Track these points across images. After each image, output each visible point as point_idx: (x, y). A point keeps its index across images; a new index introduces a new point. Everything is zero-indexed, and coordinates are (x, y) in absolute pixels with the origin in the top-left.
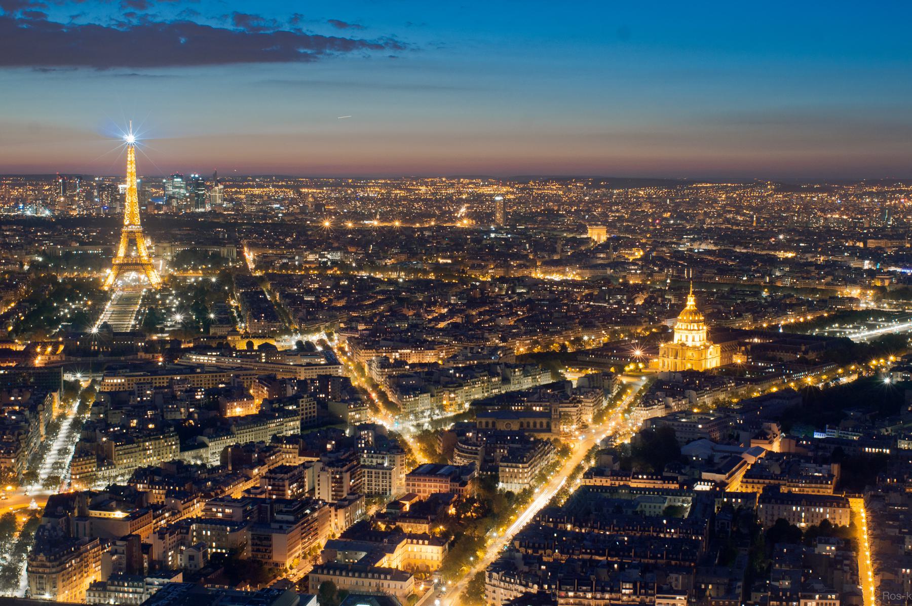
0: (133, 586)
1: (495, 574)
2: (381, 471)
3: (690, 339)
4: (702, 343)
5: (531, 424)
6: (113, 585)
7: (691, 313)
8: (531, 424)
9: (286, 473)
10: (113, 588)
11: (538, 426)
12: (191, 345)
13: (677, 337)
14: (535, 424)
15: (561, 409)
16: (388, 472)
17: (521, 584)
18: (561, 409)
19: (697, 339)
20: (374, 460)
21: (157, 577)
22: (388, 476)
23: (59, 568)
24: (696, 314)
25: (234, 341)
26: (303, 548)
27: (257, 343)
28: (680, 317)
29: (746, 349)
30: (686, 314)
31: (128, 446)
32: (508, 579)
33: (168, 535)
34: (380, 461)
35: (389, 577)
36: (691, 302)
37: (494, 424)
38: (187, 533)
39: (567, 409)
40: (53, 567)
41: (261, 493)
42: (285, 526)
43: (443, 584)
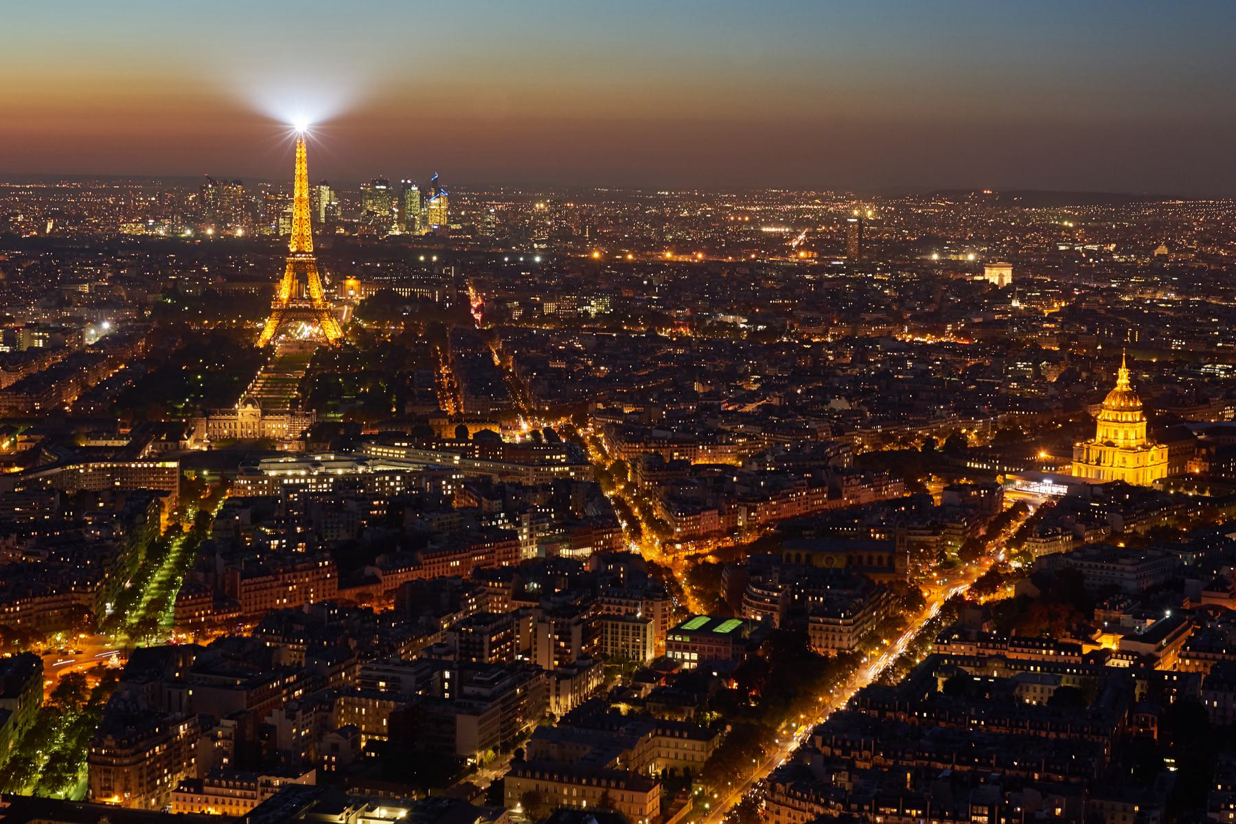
0: (241, 788)
1: (779, 785)
2: (631, 625)
3: (1121, 435)
4: (1140, 442)
5: (865, 559)
6: (211, 784)
7: (1124, 395)
8: (865, 559)
9: (486, 624)
10: (212, 789)
11: (875, 563)
12: (376, 432)
13: (1100, 433)
14: (870, 558)
15: (912, 538)
16: (642, 626)
17: (817, 802)
18: (912, 538)
19: (1132, 436)
20: (623, 608)
21: (278, 776)
22: (642, 633)
23: (133, 759)
24: (1130, 398)
25: (439, 427)
26: (503, 737)
27: (472, 431)
28: (1106, 403)
29: (1208, 452)
30: (1115, 397)
31: (260, 579)
32: (798, 794)
33: (300, 713)
34: (631, 609)
35: (622, 784)
36: (1123, 378)
37: (808, 557)
38: (331, 710)
39: (922, 538)
40: (126, 756)
41: (447, 654)
42: (476, 704)
43: (706, 799)
